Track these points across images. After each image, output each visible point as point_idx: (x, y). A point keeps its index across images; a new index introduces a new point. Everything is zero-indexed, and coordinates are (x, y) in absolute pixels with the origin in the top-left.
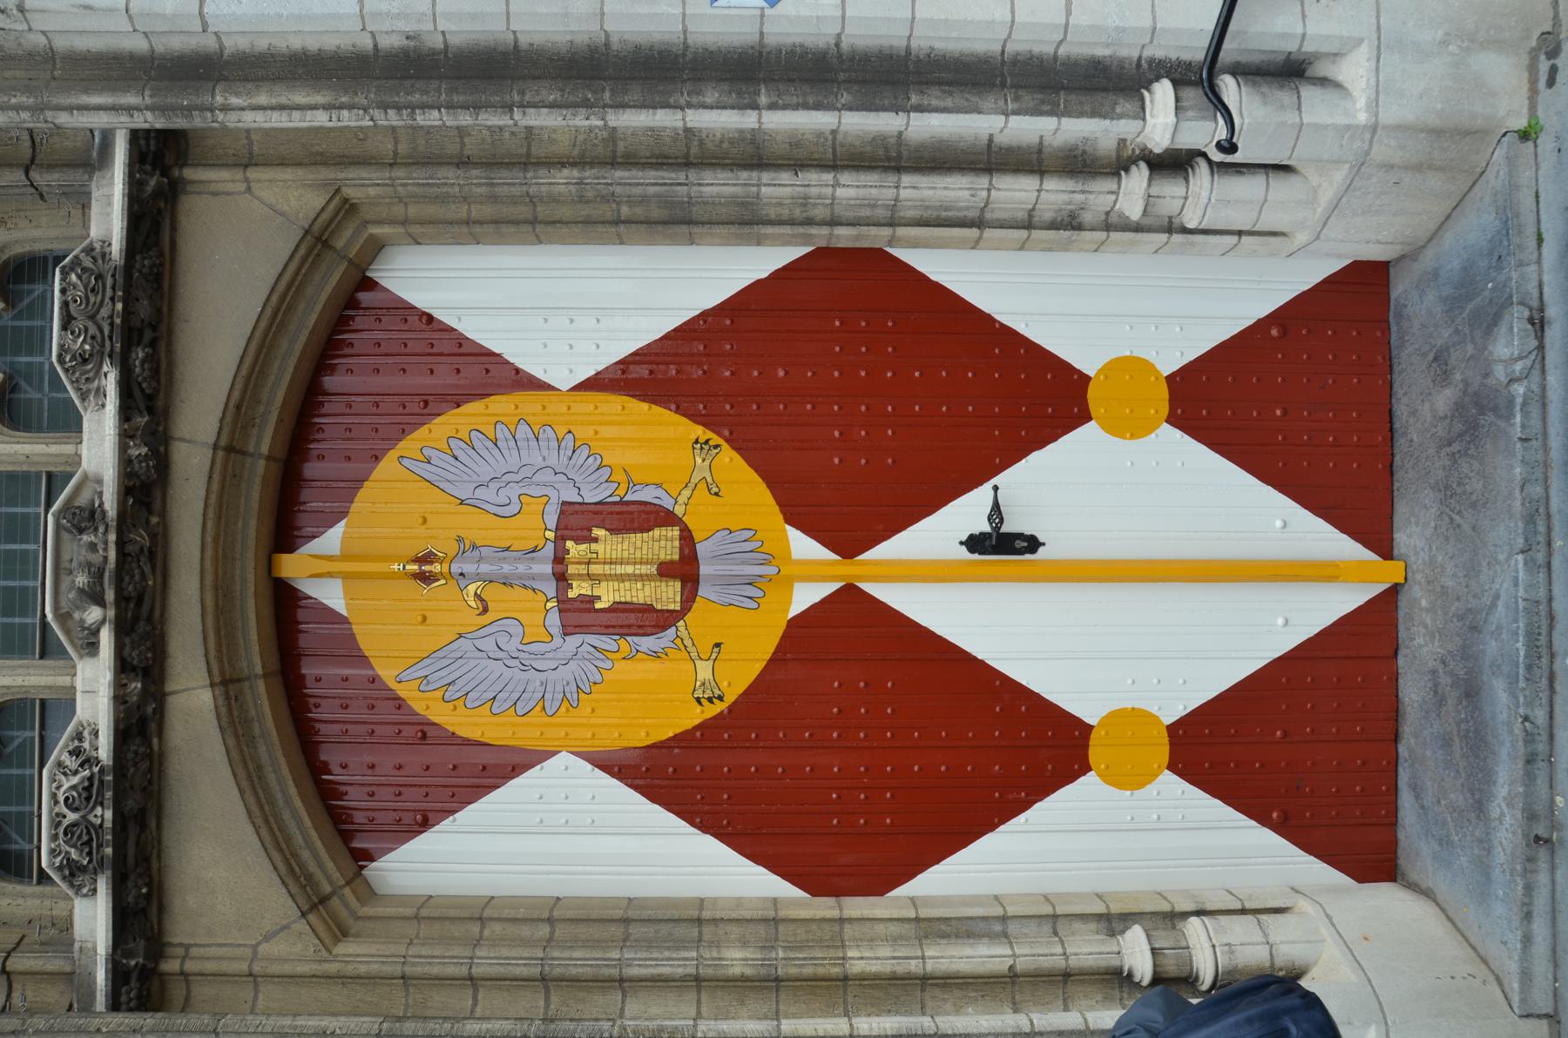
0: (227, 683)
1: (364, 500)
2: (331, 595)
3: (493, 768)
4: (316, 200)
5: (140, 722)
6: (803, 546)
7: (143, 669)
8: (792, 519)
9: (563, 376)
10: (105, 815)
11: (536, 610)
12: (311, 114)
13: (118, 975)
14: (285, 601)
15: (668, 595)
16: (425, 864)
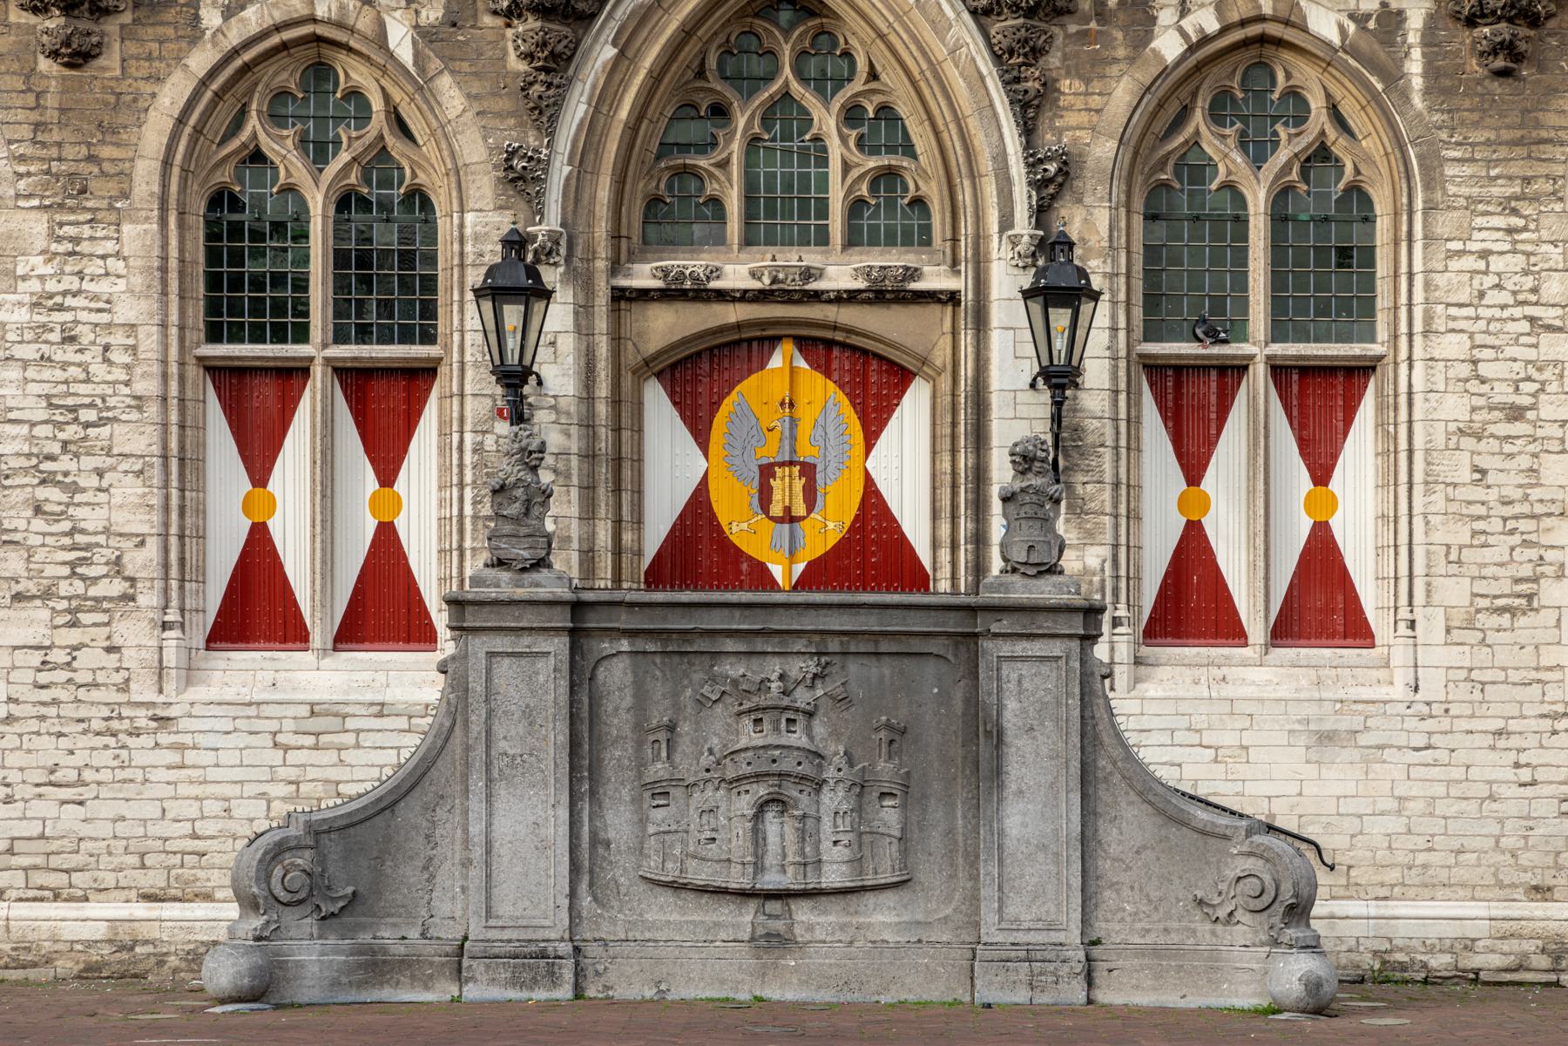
0: (739, 326)
1: (819, 378)
2: (777, 361)
3: (701, 436)
4: (938, 363)
5: (722, 296)
6: (799, 568)
7: (745, 297)
8: (809, 564)
9: (869, 465)
10: (688, 285)
11: (771, 451)
12: (967, 369)
13: (623, 290)
14: (775, 340)
15: (776, 510)
16: (658, 404)
